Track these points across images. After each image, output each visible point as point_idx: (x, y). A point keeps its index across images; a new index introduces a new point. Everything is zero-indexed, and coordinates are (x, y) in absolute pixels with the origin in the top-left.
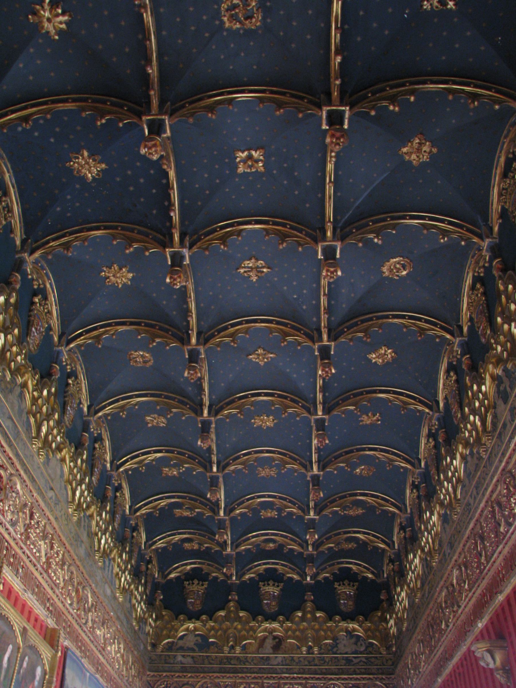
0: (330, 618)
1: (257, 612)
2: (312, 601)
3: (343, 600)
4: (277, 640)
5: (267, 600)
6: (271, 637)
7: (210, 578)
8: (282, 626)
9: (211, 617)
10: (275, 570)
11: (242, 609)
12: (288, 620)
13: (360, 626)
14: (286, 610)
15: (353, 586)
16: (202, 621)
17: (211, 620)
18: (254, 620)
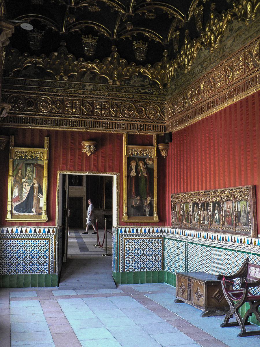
0: (129, 63)
1: (79, 54)
2: (117, 51)
3: (138, 53)
4: (94, 75)
5: (87, 47)
6: (88, 72)
7: (47, 28)
8: (97, 66)
9: (48, 56)
10: (94, 28)
11: (70, 52)
12: (101, 63)
13: (148, 71)
14: (100, 55)
15: (145, 44)
16: (42, 58)
17: (48, 57)
18: (77, 60)
